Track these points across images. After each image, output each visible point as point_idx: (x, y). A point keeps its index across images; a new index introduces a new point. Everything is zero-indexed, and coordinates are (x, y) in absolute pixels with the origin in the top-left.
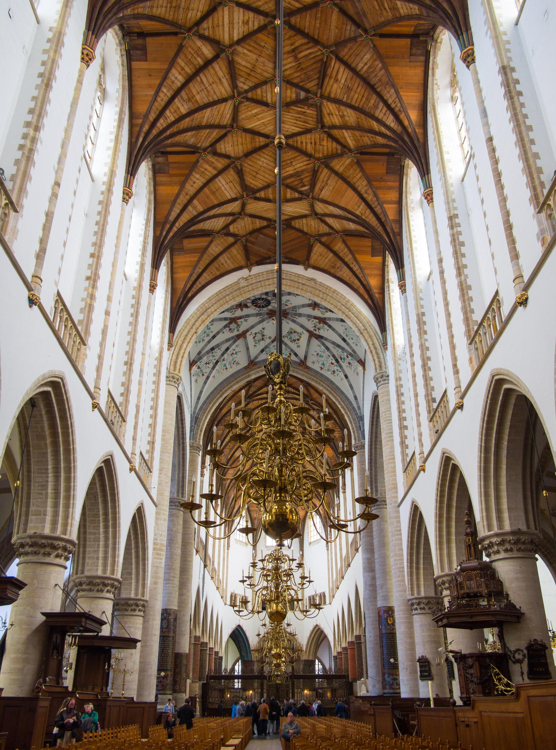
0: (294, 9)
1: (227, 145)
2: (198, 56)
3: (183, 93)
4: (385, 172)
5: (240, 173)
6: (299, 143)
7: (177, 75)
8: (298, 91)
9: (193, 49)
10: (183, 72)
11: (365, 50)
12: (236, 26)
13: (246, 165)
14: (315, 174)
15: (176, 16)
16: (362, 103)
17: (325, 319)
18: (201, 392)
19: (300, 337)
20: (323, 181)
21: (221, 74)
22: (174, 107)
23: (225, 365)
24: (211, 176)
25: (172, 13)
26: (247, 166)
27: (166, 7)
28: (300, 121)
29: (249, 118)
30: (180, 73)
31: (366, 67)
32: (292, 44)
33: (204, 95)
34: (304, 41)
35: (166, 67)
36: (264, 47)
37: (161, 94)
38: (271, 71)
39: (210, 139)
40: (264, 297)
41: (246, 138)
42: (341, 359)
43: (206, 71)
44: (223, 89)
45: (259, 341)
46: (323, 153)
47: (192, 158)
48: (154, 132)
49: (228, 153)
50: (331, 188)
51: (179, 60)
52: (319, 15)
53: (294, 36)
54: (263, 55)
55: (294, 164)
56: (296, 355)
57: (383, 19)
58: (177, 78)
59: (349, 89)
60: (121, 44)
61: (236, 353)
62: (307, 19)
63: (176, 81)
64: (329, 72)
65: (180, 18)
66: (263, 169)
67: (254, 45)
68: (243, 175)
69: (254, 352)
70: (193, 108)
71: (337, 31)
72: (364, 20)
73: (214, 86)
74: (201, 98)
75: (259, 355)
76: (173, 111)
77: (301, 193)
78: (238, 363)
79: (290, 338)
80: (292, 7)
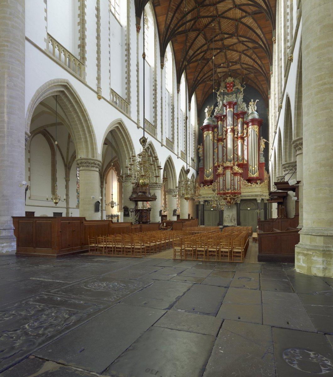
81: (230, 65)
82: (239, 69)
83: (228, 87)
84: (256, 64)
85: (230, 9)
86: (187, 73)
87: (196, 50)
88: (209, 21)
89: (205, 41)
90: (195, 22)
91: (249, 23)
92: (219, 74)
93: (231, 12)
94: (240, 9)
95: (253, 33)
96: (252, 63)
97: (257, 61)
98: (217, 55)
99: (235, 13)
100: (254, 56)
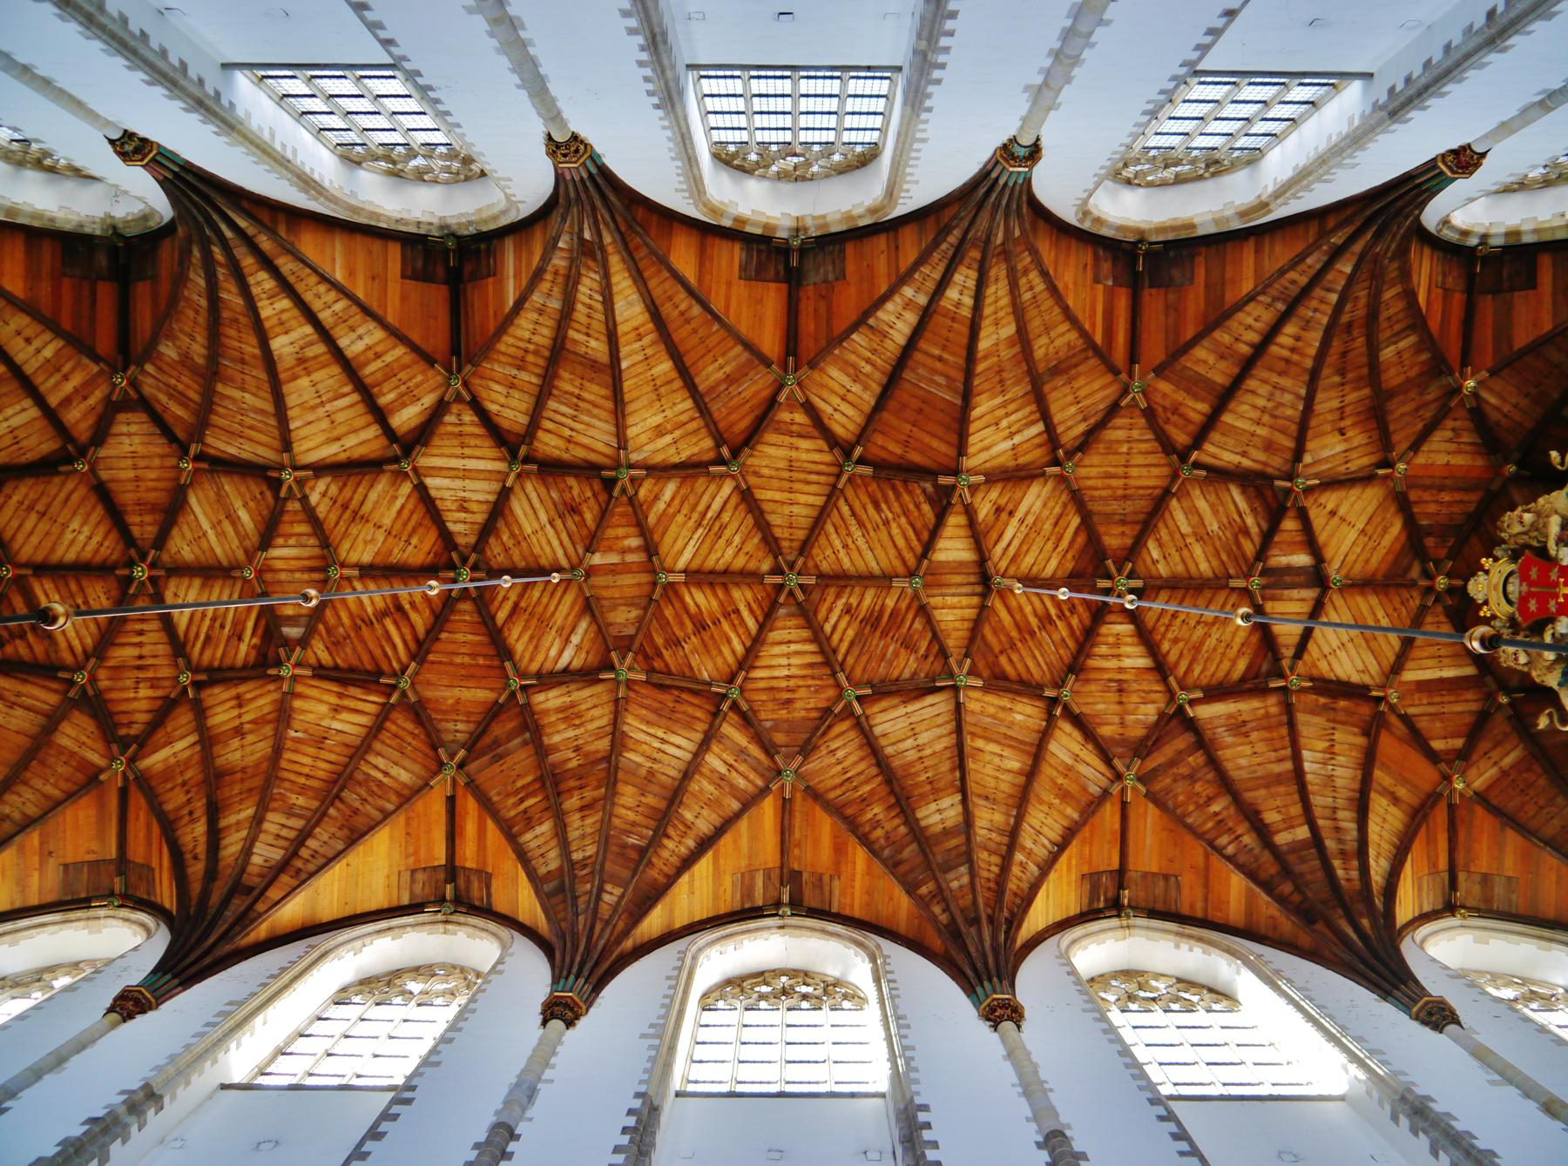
0: (493, 609)
1: (137, 440)
2: (402, 395)
3: (320, 349)
4: (69, 860)
5: (44, 468)
7: (367, 340)
8: (303, 620)
9: (417, 386)
10: (370, 354)
11: (417, 768)
12: (458, 483)
13: (70, 485)
15: (503, 359)
16: (292, 777)
20: (18, 695)
21: (351, 441)
22: (294, 323)
24: (42, 389)
25: (512, 351)
26: (68, 490)
27: (529, 341)
28: (211, 627)
29: (221, 498)
30: (369, 348)
31: (379, 776)
32: (412, 604)
33: (306, 397)
34: (421, 630)
35: (390, 319)
36: (408, 542)
37: (333, 295)
38: (354, 557)
39: (163, 398)
43: (361, 408)
44: (313, 445)
46: (110, 689)
47: (105, 341)
48: (248, 262)
49: (112, 440)
51: (400, 351)
52: (481, 661)
53: (432, 610)
54: (391, 539)
57: (496, 799)
58: (359, 340)
59: (320, 742)
60: (442, 227)
62: (470, 637)
63: (353, 336)
64: (353, 691)
65: (496, 367)
66: (56, 530)
67: (412, 523)
68: (37, 476)
70: (280, 367)
71: (450, 701)
72: (485, 759)
73: (325, 424)
74: (299, 392)
76: (285, 316)
80: (496, 603)
81: (1302, 559)
82: (1402, 503)
83: (1543, 600)
84: (1274, 349)
85: (746, 497)
86: (1199, 914)
87: (958, 774)
88: (805, 641)
89: (930, 699)
90: (747, 721)
91: (856, 388)
92: (1409, 676)
93: (778, 496)
94: (751, 438)
95: (918, 356)
96: (1285, 382)
97: (1254, 337)
98: (1165, 646)
99: (786, 475)
100: (1208, 362)
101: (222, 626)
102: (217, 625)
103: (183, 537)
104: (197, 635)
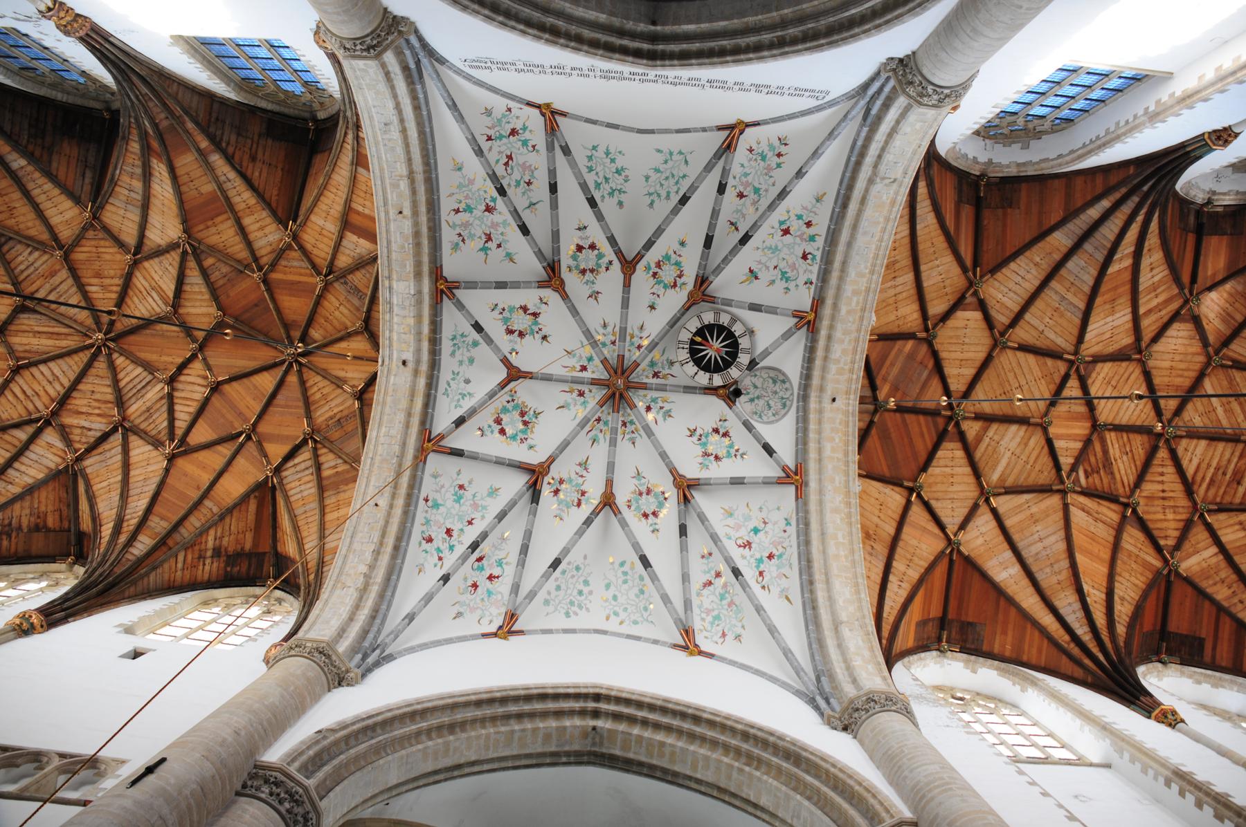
5: (1118, 357)
6: (1160, 470)
14: (1112, 498)
17: (616, 512)
18: (460, 118)
19: (514, 437)
20: (1097, 513)
23: (469, 209)
28: (1214, 474)
40: (744, 359)
41: (1181, 376)
42: (480, 559)
45: (506, 320)
50: (1092, 529)
55: (1125, 458)
56: (460, 422)
61: (484, 249)
69: (478, 302)
75: (469, 315)
77: (1074, 468)
78: (456, 247)
79: (505, 410)
101: (1224, 474)
102: (1221, 472)
103: (1196, 410)
104: (1203, 478)
